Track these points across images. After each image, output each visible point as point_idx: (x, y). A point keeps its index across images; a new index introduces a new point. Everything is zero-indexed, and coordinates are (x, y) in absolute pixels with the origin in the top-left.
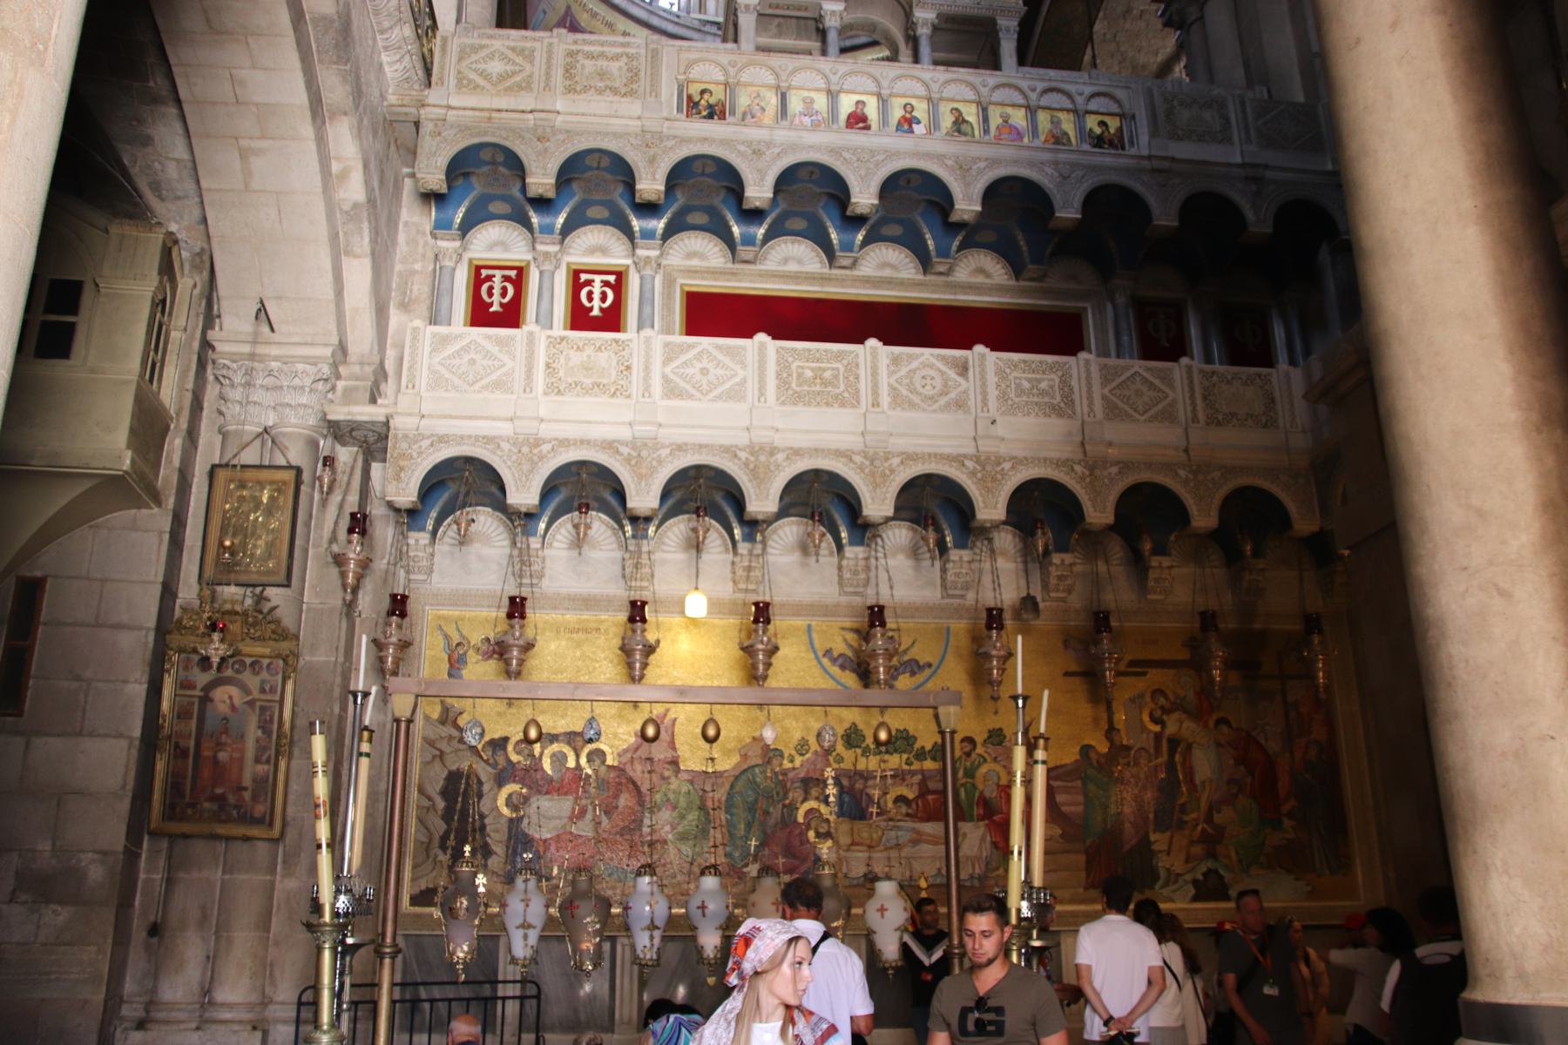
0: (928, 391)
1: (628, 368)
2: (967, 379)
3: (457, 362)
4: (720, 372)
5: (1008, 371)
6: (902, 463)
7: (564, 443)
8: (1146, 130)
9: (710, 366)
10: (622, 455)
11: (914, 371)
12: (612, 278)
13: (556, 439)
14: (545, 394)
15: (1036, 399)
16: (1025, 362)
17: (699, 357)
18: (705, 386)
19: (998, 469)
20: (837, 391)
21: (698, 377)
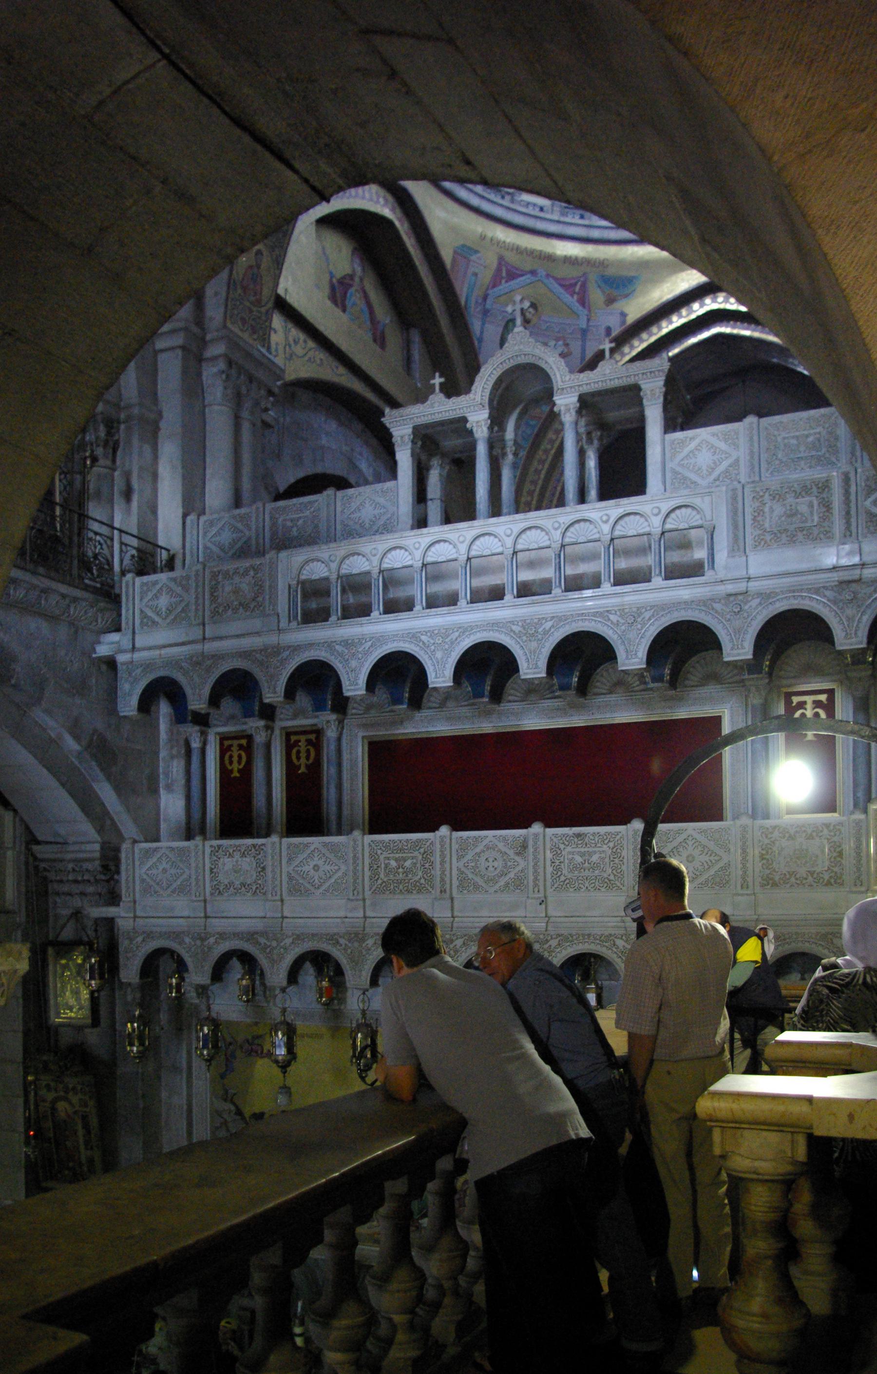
0: (491, 873)
1: (264, 869)
2: (525, 859)
3: (154, 871)
4: (328, 868)
5: (562, 846)
6: (464, 943)
7: (222, 936)
8: (725, 544)
9: (321, 863)
10: (260, 944)
11: (478, 855)
12: (313, 737)
13: (218, 933)
14: (212, 894)
15: (587, 873)
16: (578, 835)
17: (311, 856)
18: (316, 881)
19: (546, 946)
20: (416, 878)
21: (312, 872)
